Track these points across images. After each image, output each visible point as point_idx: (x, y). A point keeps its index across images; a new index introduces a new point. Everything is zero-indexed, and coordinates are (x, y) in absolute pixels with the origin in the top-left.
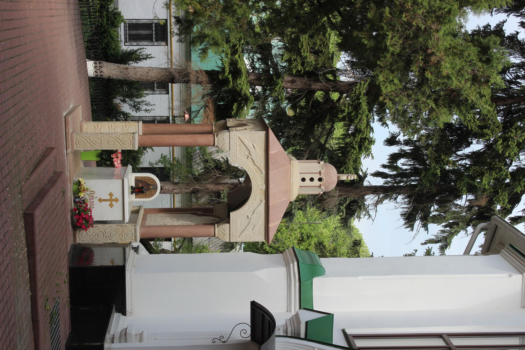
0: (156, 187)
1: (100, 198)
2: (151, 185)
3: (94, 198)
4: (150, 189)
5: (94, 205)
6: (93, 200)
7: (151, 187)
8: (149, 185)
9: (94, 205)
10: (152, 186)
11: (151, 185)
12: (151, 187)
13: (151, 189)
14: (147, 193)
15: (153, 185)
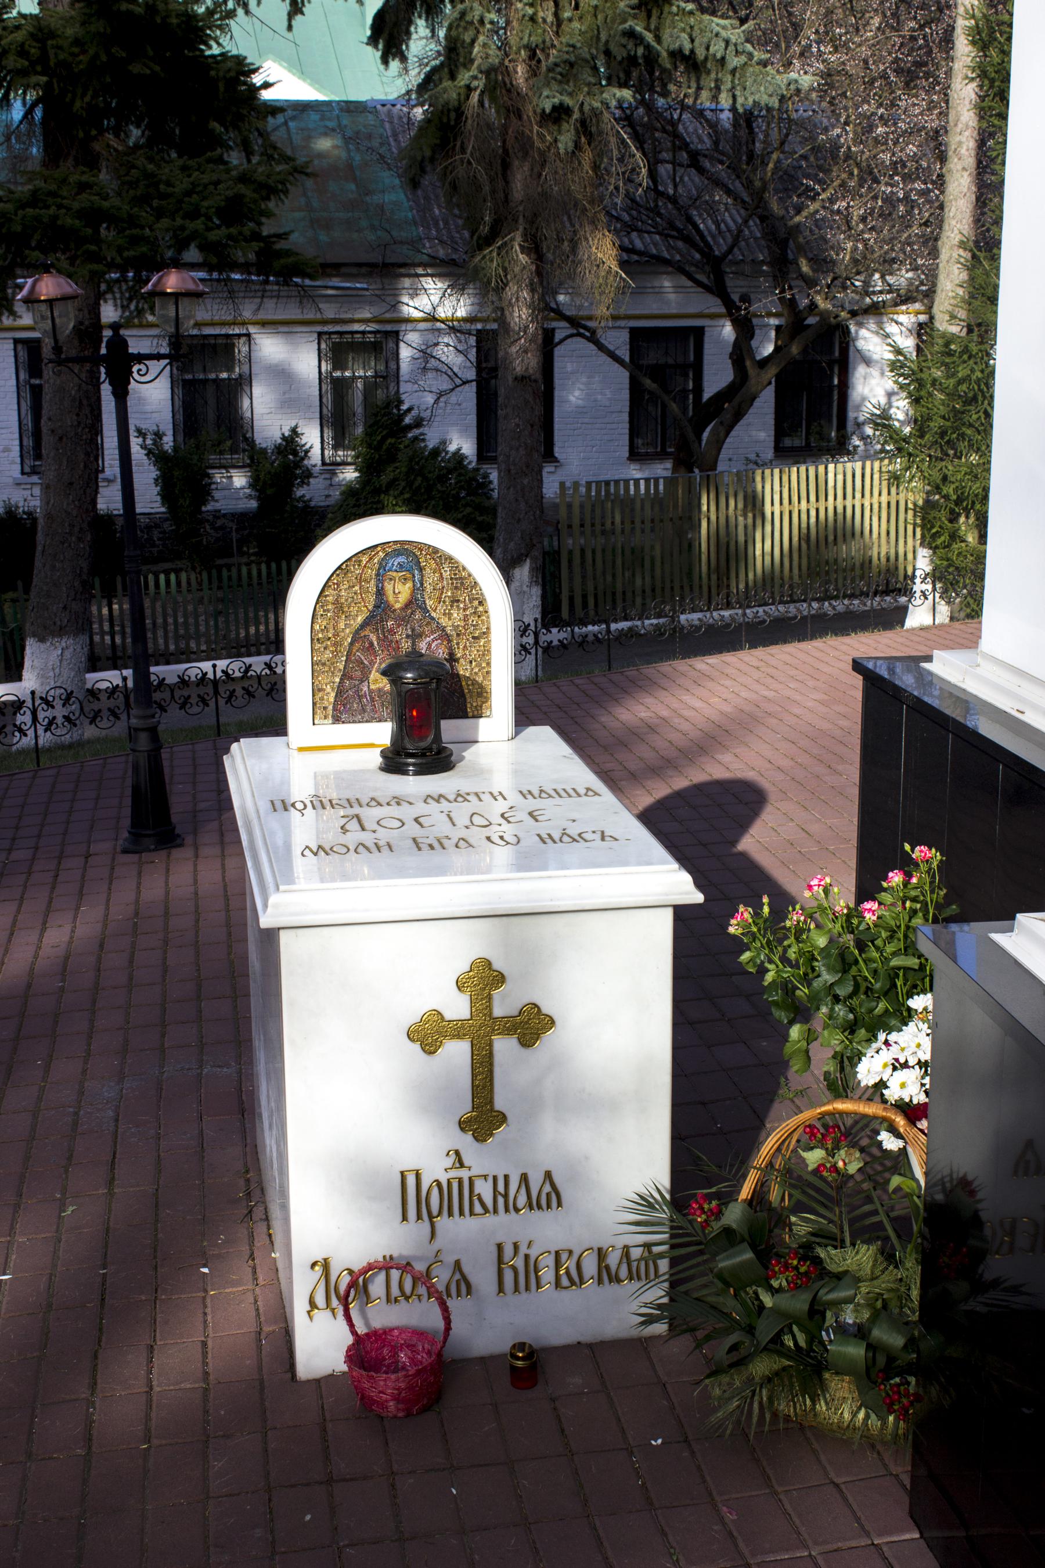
0: (397, 553)
1: (463, 1125)
2: (380, 592)
3: (464, 1174)
4: (414, 603)
5: (524, 1178)
6: (484, 1189)
7: (399, 592)
8: (381, 608)
9: (524, 1178)
10: (389, 587)
11: (380, 592)
12: (399, 592)
13: (418, 589)
14: (444, 621)
15: (380, 577)
